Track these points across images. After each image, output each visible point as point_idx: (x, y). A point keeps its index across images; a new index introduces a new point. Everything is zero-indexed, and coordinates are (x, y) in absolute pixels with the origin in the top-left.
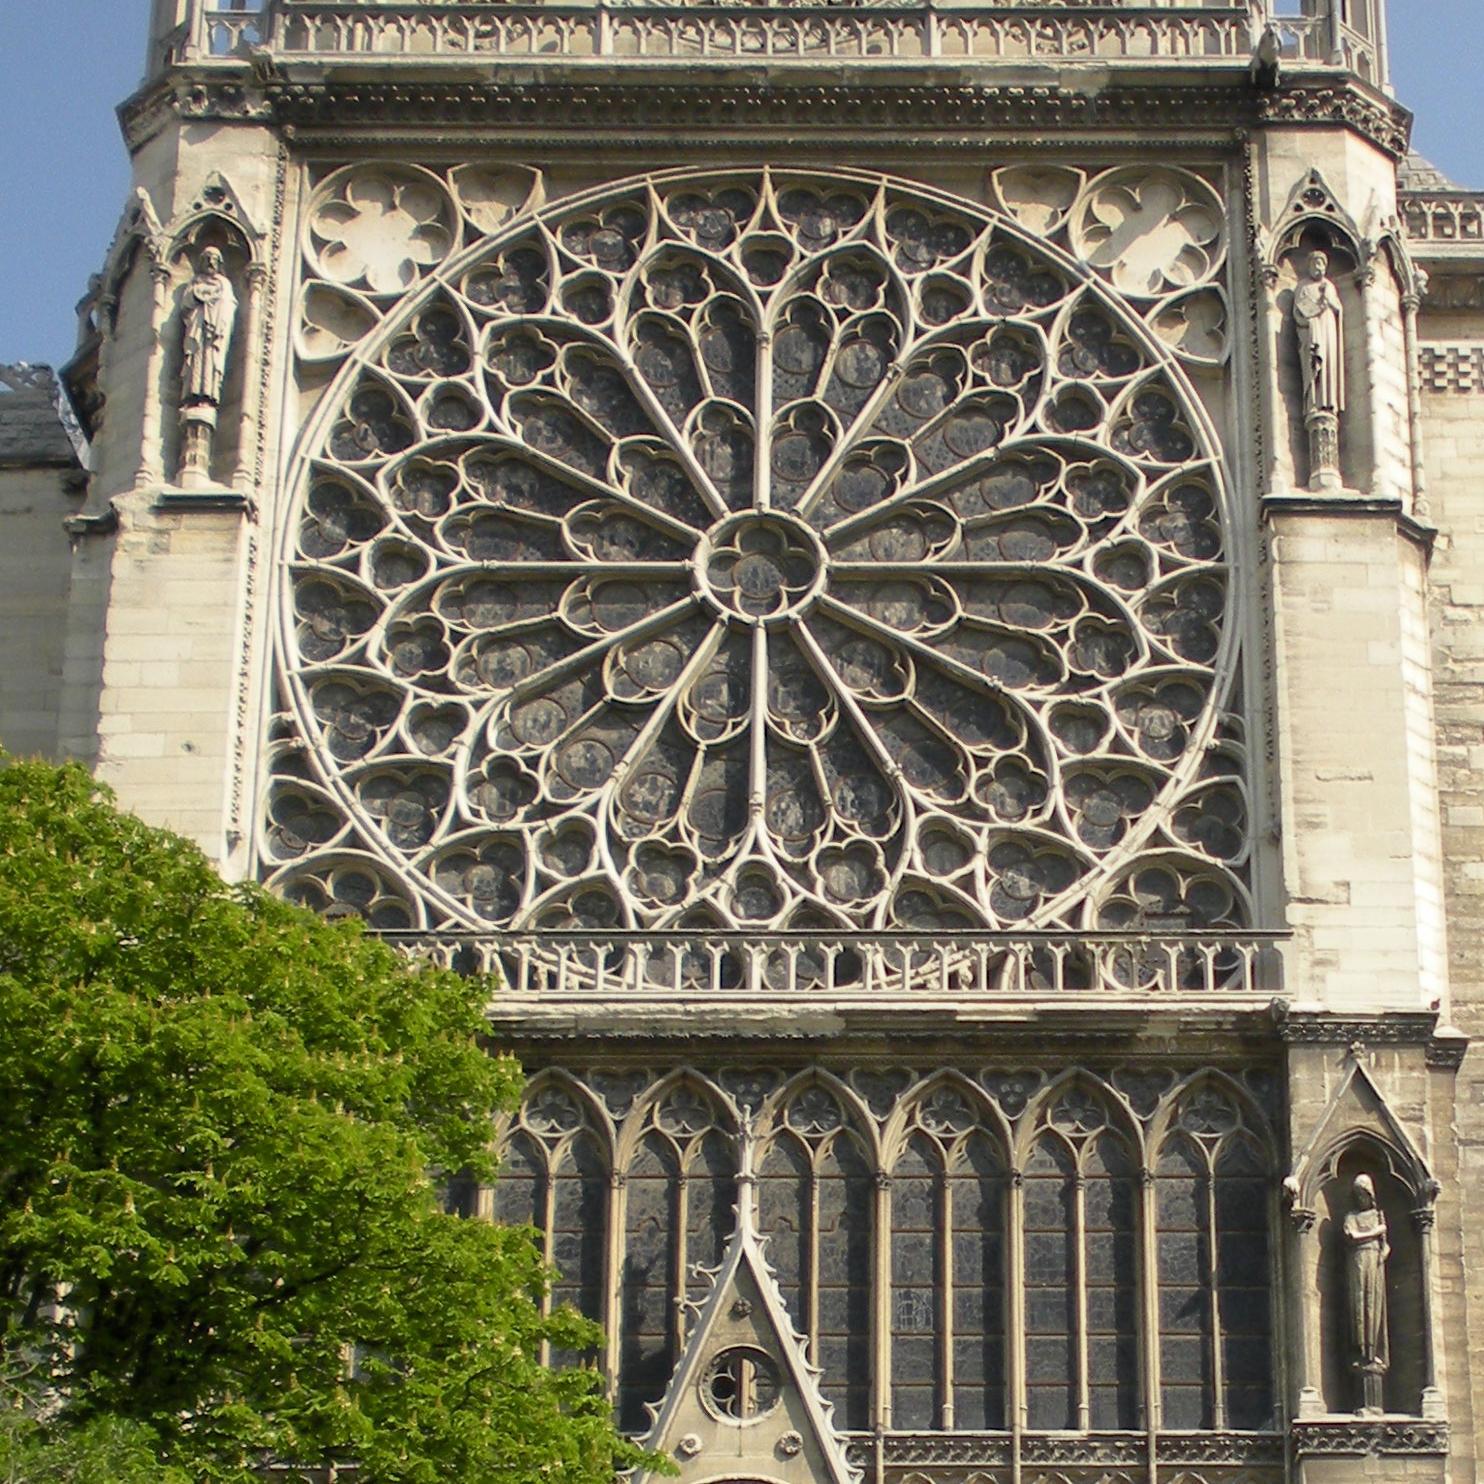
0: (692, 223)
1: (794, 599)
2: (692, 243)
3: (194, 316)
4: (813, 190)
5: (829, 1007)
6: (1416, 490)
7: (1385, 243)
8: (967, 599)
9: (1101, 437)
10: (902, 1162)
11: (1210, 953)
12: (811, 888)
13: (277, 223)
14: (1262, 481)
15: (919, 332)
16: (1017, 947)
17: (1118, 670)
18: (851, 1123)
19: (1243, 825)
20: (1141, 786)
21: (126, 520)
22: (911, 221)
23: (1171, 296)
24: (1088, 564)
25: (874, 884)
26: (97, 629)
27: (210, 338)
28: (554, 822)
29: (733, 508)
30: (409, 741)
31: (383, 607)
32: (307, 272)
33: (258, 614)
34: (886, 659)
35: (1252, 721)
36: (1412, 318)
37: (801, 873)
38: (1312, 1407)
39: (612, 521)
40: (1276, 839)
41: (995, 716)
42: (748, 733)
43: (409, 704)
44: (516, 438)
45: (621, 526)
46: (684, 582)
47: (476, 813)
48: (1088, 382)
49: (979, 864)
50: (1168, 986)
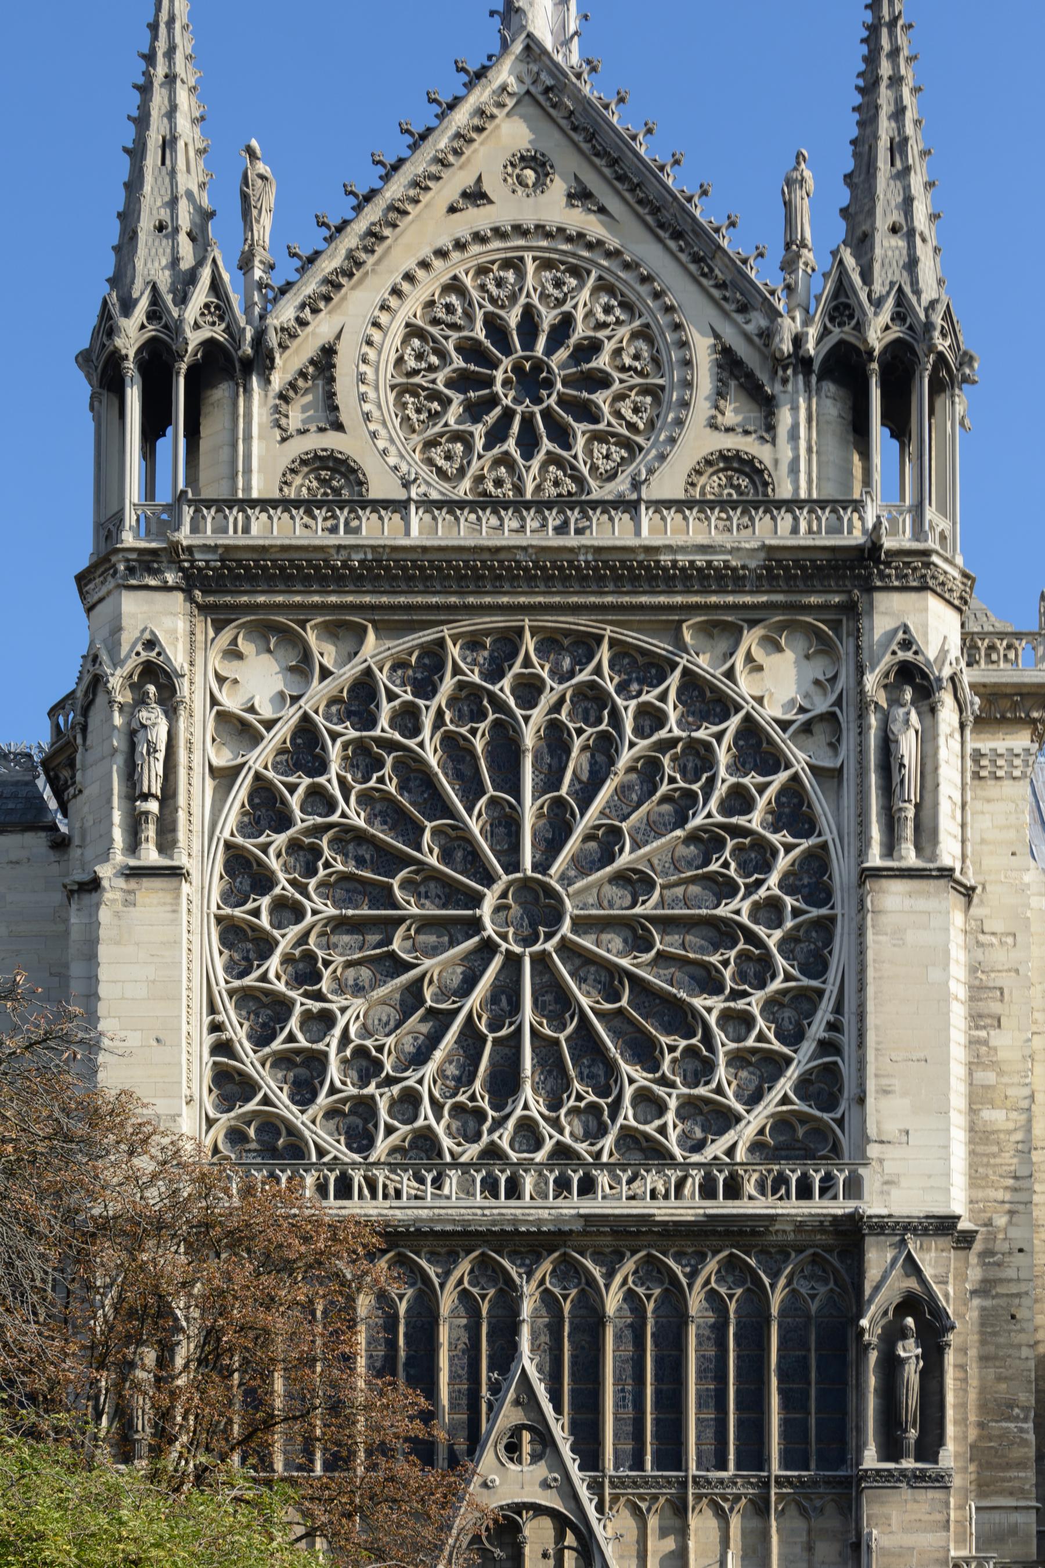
0: (474, 662)
1: (549, 937)
2: (476, 678)
3: (141, 735)
4: (559, 637)
5: (573, 1212)
6: (964, 857)
7: (952, 679)
8: (664, 933)
9: (755, 820)
10: (620, 1309)
11: (817, 1177)
12: (561, 1132)
13: (192, 664)
14: (862, 853)
15: (632, 745)
16: (694, 1172)
17: (762, 986)
18: (588, 1284)
19: (841, 1090)
20: (776, 1065)
21: (105, 883)
22: (626, 661)
23: (802, 718)
24: (745, 913)
25: (602, 1131)
26: (91, 957)
27: (152, 750)
28: (396, 1089)
29: (507, 873)
30: (300, 1036)
31: (277, 943)
32: (214, 702)
33: (196, 948)
34: (609, 979)
35: (848, 1020)
36: (968, 731)
37: (555, 1124)
38: (870, 1459)
39: (427, 881)
40: (862, 1100)
41: (682, 1019)
42: (519, 1030)
43: (298, 1010)
44: (361, 823)
45: (432, 885)
46: (475, 925)
47: (344, 1083)
48: (746, 781)
49: (670, 1117)
50: (788, 1197)
